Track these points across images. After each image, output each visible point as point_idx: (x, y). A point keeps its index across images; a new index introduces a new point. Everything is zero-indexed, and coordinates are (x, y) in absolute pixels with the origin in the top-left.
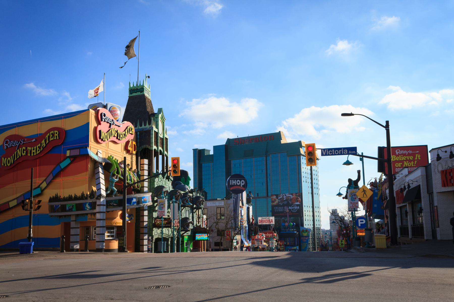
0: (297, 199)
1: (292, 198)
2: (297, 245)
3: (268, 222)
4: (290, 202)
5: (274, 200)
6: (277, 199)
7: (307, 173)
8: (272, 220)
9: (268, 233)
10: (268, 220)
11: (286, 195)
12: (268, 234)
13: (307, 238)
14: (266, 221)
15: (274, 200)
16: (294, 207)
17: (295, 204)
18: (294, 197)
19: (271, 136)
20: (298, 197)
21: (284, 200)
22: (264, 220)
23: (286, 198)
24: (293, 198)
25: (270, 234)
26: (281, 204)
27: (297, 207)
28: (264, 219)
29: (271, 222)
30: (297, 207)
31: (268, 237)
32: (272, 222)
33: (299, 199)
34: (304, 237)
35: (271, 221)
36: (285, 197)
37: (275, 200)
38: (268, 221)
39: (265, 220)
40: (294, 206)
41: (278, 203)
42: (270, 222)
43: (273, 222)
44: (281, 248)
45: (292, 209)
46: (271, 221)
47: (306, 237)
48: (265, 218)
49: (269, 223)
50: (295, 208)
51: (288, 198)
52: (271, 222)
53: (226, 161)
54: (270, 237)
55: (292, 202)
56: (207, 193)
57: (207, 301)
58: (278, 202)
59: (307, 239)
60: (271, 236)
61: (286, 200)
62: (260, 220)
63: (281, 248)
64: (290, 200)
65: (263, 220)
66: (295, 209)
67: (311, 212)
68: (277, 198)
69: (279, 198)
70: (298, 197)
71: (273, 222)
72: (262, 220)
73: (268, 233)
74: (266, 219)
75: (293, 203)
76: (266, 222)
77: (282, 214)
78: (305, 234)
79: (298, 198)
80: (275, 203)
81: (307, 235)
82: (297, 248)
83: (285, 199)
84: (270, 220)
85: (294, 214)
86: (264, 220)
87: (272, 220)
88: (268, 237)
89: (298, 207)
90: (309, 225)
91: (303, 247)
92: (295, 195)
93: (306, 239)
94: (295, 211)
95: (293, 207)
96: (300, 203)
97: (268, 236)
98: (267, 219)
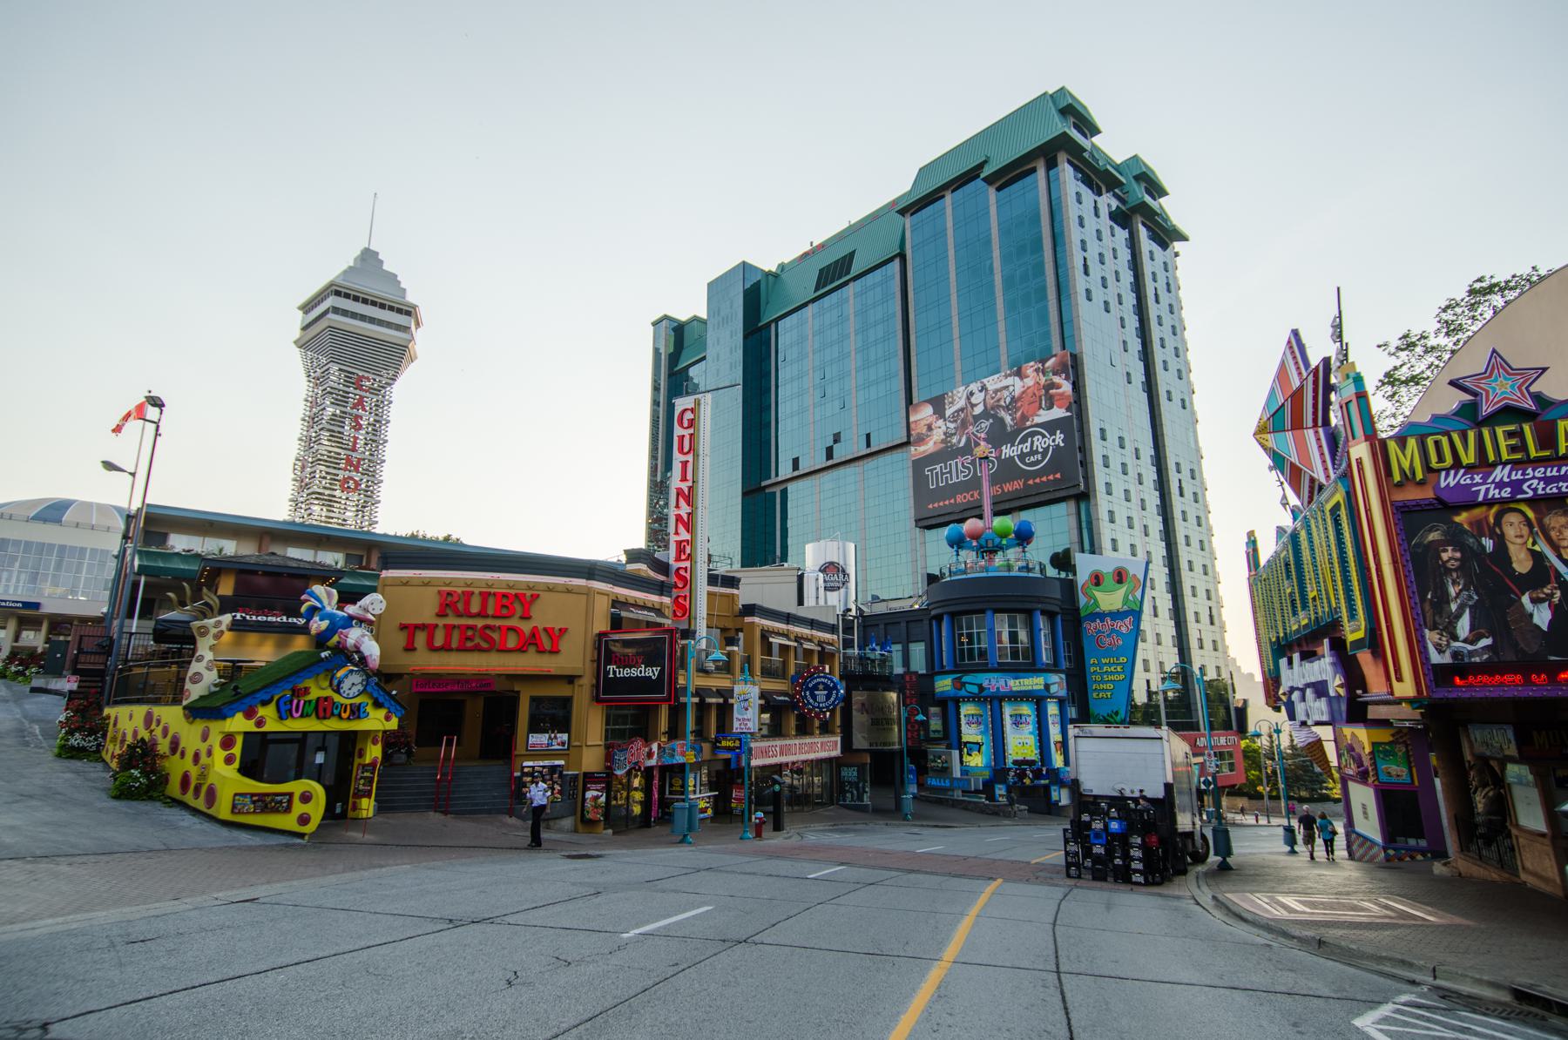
0: (1047, 392)
1: (1017, 394)
2: (1054, 668)
4: (1008, 419)
5: (924, 431)
6: (940, 422)
11: (983, 388)
13: (1124, 626)
15: (924, 430)
16: (1032, 442)
17: (1037, 425)
18: (1029, 382)
20: (1057, 379)
21: (974, 417)
23: (984, 400)
24: (1023, 392)
26: (959, 442)
27: (1052, 433)
30: (1052, 433)
33: (1058, 386)
34: (1102, 616)
36: (978, 398)
37: (930, 428)
40: (1033, 434)
41: (943, 441)
45: (1022, 456)
47: (1117, 615)
50: (1039, 443)
51: (999, 400)
55: (1019, 414)
58: (945, 434)
59: (1124, 630)
61: (985, 414)
64: (1007, 408)
66: (1037, 452)
68: (939, 411)
69: (948, 412)
70: (1057, 379)
75: (1024, 418)
77: (968, 497)
78: (1110, 599)
79: (1053, 385)
80: (931, 444)
81: (1126, 600)
82: (1047, 686)
83: (978, 410)
85: (1031, 482)
89: (1059, 438)
91: (1103, 682)
92: (1037, 370)
93: (1119, 633)
94: (1038, 462)
95: (1023, 441)
96: (1068, 410)
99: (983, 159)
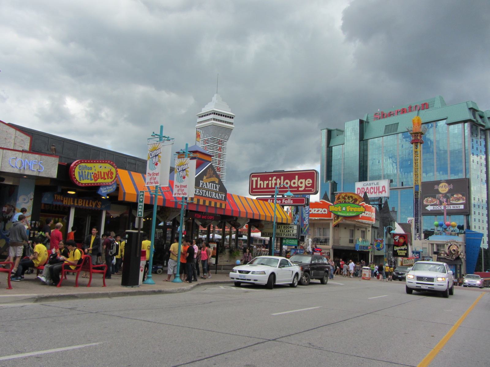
3: (376, 193)
7: (479, 163)
8: (384, 187)
9: (297, 177)
10: (377, 187)
12: (296, 181)
14: (372, 190)
19: (424, 104)
22: (367, 188)
25: (303, 181)
28: (367, 186)
29: (383, 191)
31: (298, 191)
32: (384, 193)
35: (381, 190)
38: (375, 191)
39: (369, 187)
42: (379, 192)
43: (385, 192)
44: (401, 250)
46: (381, 190)
48: (370, 184)
49: (377, 193)
52: (381, 192)
53: (360, 141)
54: (304, 190)
56: (337, 184)
57: (180, 366)
60: (306, 187)
62: (358, 189)
63: (401, 250)
65: (365, 188)
67: (486, 223)
71: (385, 192)
72: (362, 188)
73: (297, 177)
74: (372, 186)
76: (372, 193)
84: (379, 187)
86: (367, 188)
87: (384, 187)
88: (298, 191)
90: (481, 228)
97: (298, 187)
98: (373, 186)
99: (446, 118)
